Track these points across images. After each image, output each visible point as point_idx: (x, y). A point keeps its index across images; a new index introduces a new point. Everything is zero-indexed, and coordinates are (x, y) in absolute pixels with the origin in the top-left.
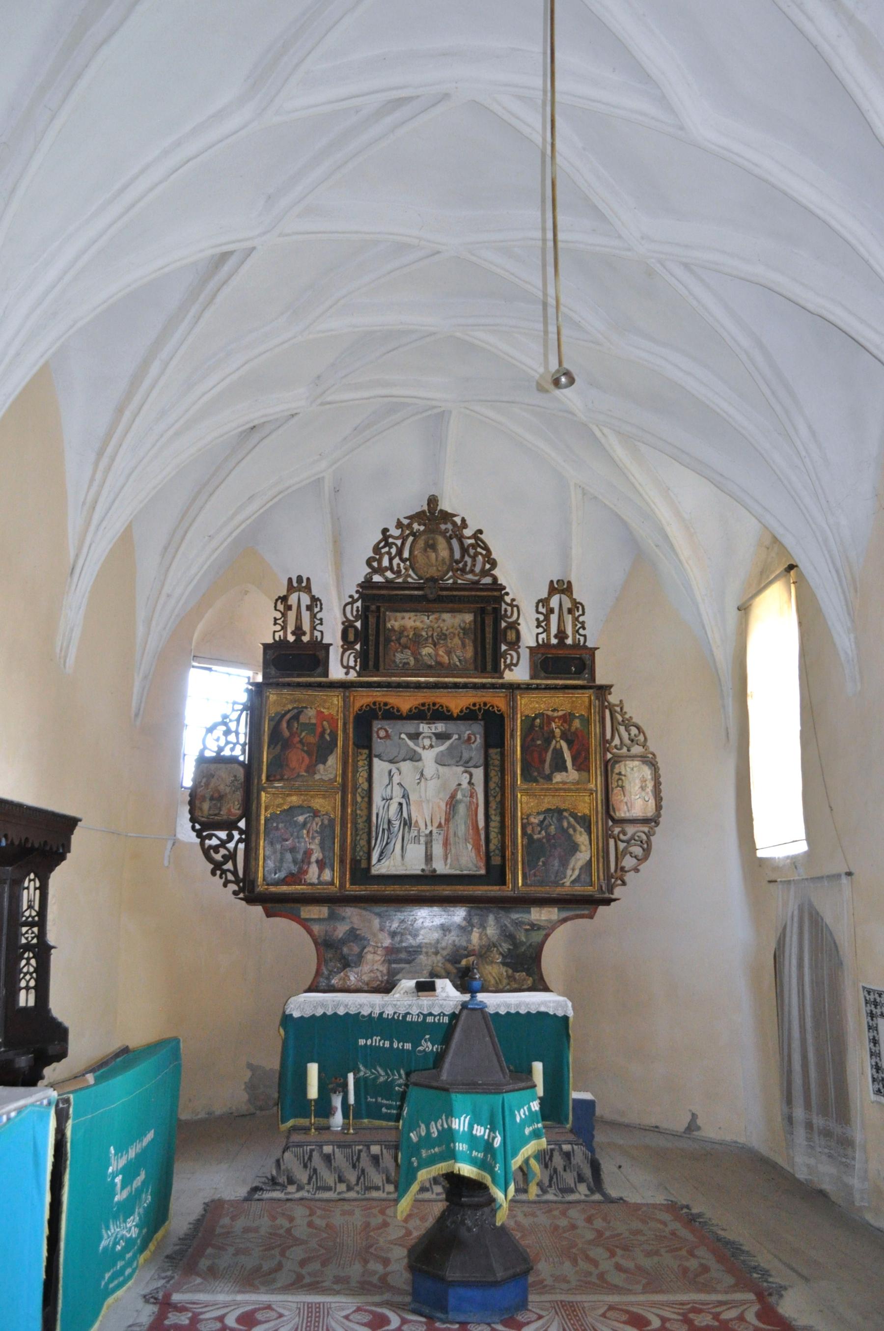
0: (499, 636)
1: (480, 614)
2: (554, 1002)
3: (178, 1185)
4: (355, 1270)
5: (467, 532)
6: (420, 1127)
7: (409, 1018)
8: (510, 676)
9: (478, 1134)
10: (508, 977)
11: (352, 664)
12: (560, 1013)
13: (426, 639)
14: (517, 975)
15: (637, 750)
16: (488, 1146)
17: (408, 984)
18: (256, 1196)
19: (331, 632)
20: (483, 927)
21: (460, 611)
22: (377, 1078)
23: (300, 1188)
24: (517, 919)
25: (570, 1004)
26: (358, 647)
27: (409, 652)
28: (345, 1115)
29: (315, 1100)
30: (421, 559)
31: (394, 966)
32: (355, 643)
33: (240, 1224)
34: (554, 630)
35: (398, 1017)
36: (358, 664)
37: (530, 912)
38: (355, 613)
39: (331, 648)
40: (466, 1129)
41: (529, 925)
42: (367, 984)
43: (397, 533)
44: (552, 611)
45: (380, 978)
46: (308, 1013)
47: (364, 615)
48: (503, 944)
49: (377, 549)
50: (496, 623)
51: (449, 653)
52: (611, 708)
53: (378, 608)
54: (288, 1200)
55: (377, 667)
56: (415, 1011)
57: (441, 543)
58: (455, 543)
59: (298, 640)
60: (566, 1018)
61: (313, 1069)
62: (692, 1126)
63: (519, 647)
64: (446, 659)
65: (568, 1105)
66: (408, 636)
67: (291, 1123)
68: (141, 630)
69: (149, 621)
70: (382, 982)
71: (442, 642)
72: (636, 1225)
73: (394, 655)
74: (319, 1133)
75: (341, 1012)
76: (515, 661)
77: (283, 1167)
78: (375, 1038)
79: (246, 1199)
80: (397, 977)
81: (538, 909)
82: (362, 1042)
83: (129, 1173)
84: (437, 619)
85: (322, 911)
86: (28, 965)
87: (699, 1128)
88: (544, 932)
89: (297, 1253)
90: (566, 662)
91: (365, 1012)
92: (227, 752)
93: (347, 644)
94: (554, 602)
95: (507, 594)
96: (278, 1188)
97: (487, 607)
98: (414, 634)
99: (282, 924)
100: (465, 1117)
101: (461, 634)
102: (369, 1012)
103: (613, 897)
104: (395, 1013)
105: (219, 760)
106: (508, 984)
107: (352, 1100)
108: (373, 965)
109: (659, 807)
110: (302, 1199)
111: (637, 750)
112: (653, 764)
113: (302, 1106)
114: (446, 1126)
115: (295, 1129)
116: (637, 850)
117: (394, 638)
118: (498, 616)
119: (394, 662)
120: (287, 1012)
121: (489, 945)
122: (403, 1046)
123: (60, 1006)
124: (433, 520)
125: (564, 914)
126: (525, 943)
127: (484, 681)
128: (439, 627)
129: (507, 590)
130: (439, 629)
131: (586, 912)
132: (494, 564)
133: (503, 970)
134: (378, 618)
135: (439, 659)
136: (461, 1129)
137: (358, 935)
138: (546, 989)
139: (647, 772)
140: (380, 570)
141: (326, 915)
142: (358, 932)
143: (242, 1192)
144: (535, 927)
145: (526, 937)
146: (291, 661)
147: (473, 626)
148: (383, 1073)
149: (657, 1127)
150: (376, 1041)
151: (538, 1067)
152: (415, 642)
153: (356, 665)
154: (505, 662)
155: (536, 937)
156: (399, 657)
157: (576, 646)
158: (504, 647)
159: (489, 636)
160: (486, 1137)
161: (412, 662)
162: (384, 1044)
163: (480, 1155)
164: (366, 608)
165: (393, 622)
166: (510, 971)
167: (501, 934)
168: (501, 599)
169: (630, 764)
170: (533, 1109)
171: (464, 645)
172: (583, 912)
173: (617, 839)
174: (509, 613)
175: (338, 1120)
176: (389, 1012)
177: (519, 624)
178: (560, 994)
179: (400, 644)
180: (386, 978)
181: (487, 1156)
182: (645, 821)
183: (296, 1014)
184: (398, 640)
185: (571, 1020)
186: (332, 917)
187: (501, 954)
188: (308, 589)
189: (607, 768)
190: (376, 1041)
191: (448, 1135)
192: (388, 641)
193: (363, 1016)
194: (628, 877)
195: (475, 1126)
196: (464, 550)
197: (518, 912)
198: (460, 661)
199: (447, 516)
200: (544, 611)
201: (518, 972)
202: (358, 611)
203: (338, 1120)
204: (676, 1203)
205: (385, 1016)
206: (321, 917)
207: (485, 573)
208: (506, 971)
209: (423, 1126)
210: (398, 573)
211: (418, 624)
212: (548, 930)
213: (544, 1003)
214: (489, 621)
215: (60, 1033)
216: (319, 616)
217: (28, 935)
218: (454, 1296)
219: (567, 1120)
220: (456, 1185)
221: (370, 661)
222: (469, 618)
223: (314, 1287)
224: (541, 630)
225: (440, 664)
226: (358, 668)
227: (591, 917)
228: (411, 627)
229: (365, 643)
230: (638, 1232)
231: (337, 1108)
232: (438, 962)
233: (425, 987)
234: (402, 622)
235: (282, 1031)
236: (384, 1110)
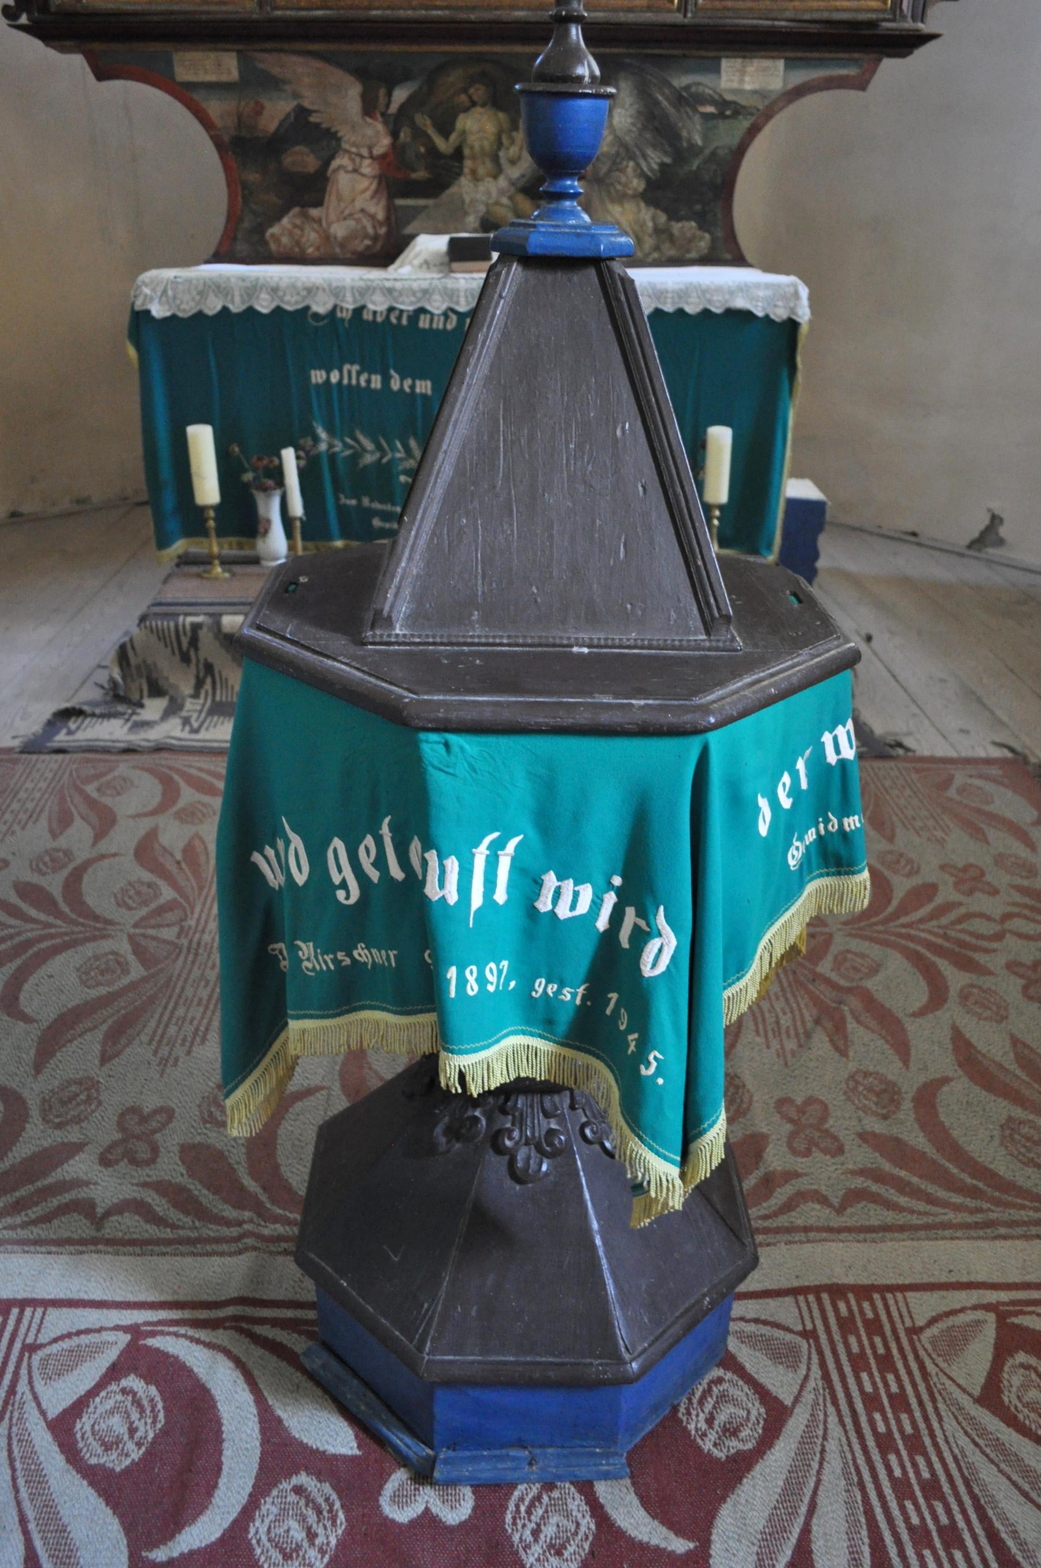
2: (767, 286)
6: (288, 842)
7: (424, 323)
9: (563, 912)
10: (657, 231)
12: (780, 314)
14: (676, 227)
16: (613, 963)
17: (431, 244)
18: (61, 738)
22: (355, 457)
23: (174, 708)
24: (687, 88)
25: (804, 292)
28: (289, 534)
29: (217, 508)
31: (400, 202)
35: (399, 318)
37: (717, 70)
40: (501, 896)
41: (712, 102)
42: (342, 246)
45: (370, 231)
46: (187, 309)
48: (650, 152)
54: (129, 750)
56: (437, 306)
60: (792, 325)
61: (202, 439)
65: (775, 513)
67: (179, 546)
70: (375, 238)
72: (961, 848)
74: (233, 575)
75: (264, 306)
77: (133, 660)
78: (346, 367)
79: (32, 747)
80: (409, 230)
81: (739, 61)
82: (318, 376)
87: (1001, 542)
88: (746, 123)
91: (321, 307)
96: (121, 708)
99: (138, 102)
100: (496, 847)
102: (329, 306)
103: (924, 28)
104: (391, 309)
106: (657, 248)
107: (297, 508)
110: (159, 749)
113: (193, 518)
114: (396, 872)
120: (137, 308)
121: (618, 154)
122: (413, 387)
125: (801, 76)
126: (701, 150)
131: (851, 71)
133: (647, 215)
136: (477, 900)
137: (317, 125)
138: (739, 260)
141: (235, 75)
142: (313, 119)
144: (728, 109)
145: (705, 137)
148: (369, 445)
149: (914, 534)
150: (349, 374)
151: (721, 438)
155: (728, 135)
160: (602, 923)
162: (368, 381)
163: (572, 995)
166: (663, 218)
167: (645, 128)
170: (832, 758)
172: (843, 72)
176: (378, 305)
178: (768, 269)
180: (383, 231)
181: (606, 1004)
183: (158, 311)
185: (804, 329)
186: (255, 82)
187: (642, 175)
190: (349, 375)
191: (405, 916)
193: (316, 316)
195: (551, 880)
197: (687, 71)
201: (679, 219)
203: (277, 543)
204: (1025, 760)
205: (367, 316)
206: (224, 78)
208: (654, 219)
209: (297, 842)
212: (757, 116)
213: (744, 289)
219: (769, 546)
227: (861, 84)
230: (970, 879)
231: (269, 522)
232: (502, 192)
235: (132, 352)
236: (377, 522)
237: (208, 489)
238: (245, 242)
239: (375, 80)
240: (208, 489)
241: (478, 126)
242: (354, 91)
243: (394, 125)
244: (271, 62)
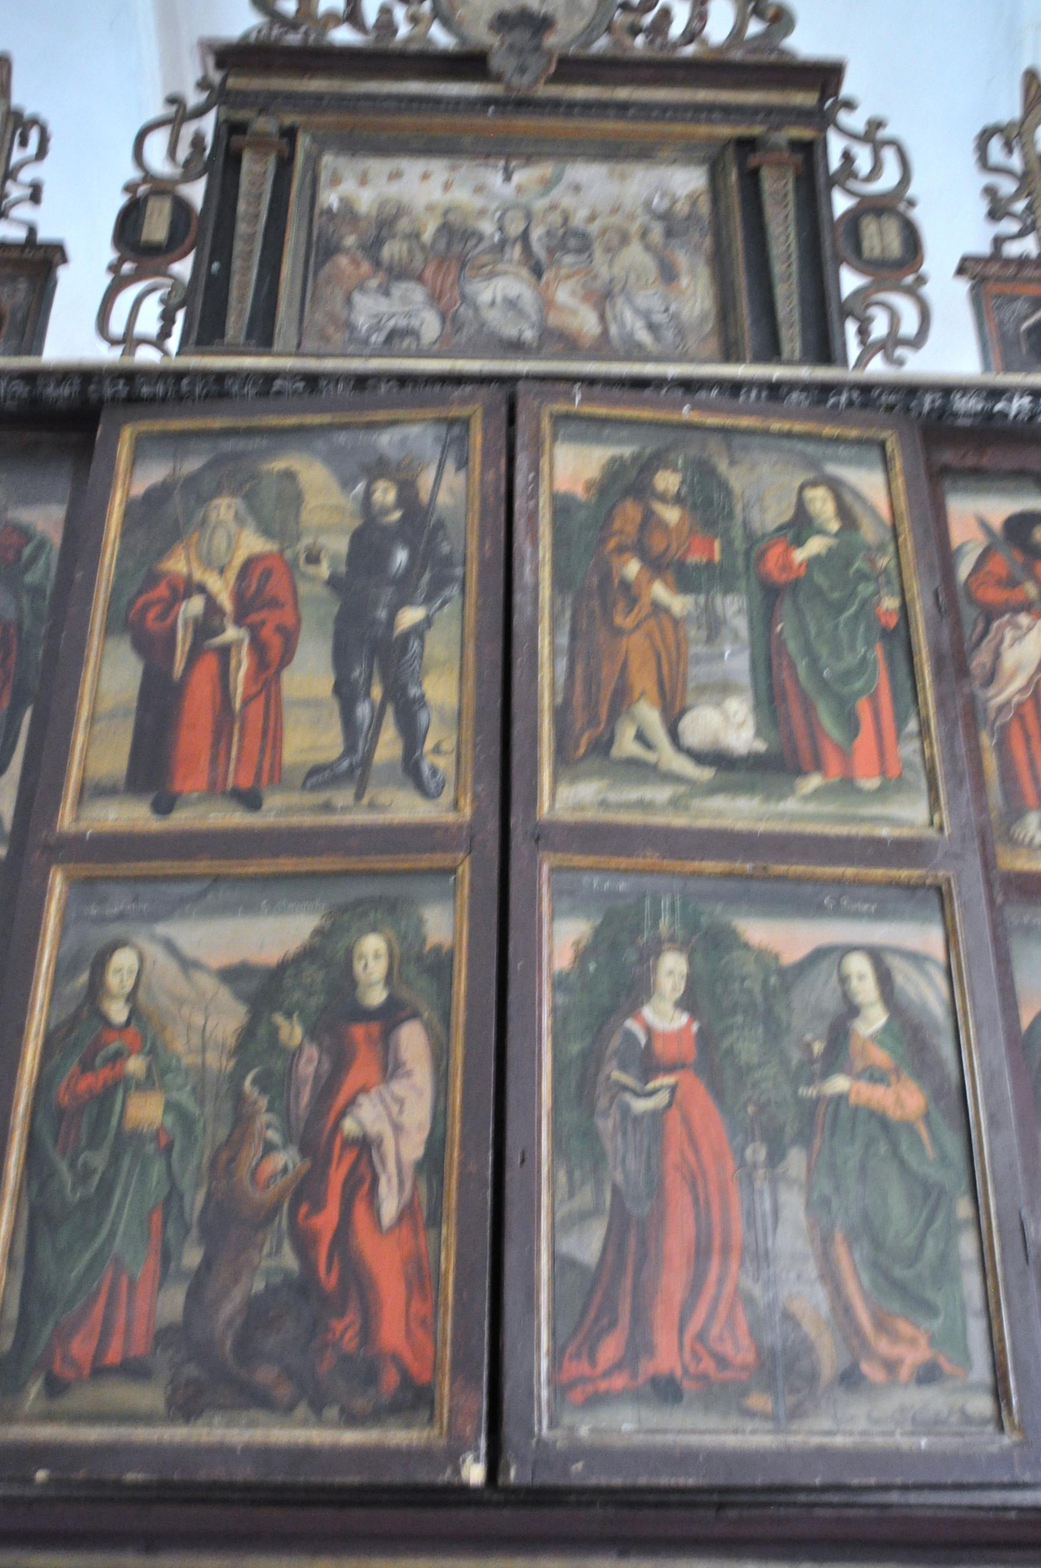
1: (738, 164)
11: (149, 322)
13: (502, 246)
21: (643, 152)
26: (183, 268)
27: (417, 294)
32: (172, 249)
36: (177, 329)
38: (183, 152)
39: (63, 274)
47: (223, 163)
51: (602, 299)
53: (290, 134)
55: (261, 334)
63: (921, 280)
64: (586, 322)
66: (416, 235)
71: (568, 259)
73: (348, 301)
76: (909, 326)
84: (548, 185)
95: (849, 105)
98: (447, 229)
101: (657, 232)
117: (350, 240)
119: (350, 326)
127: (776, 372)
128: (553, 207)
129: (847, 89)
130: (555, 218)
134: (285, 165)
135: (554, 320)
147: (704, 208)
152: (442, 261)
153: (165, 333)
154: (863, 332)
156: (369, 309)
158: (850, 281)
161: (430, 326)
165: (349, 186)
171: (668, 274)
174: (863, 161)
177: (911, 203)
179: (377, 264)
184: (372, 247)
192: (322, 250)
198: (652, 328)
200: (1016, 162)
202: (197, 142)
211: (462, 196)
216: (26, 175)
224: (1010, 226)
225: (558, 340)
226: (173, 343)
228: (430, 208)
234: (393, 190)
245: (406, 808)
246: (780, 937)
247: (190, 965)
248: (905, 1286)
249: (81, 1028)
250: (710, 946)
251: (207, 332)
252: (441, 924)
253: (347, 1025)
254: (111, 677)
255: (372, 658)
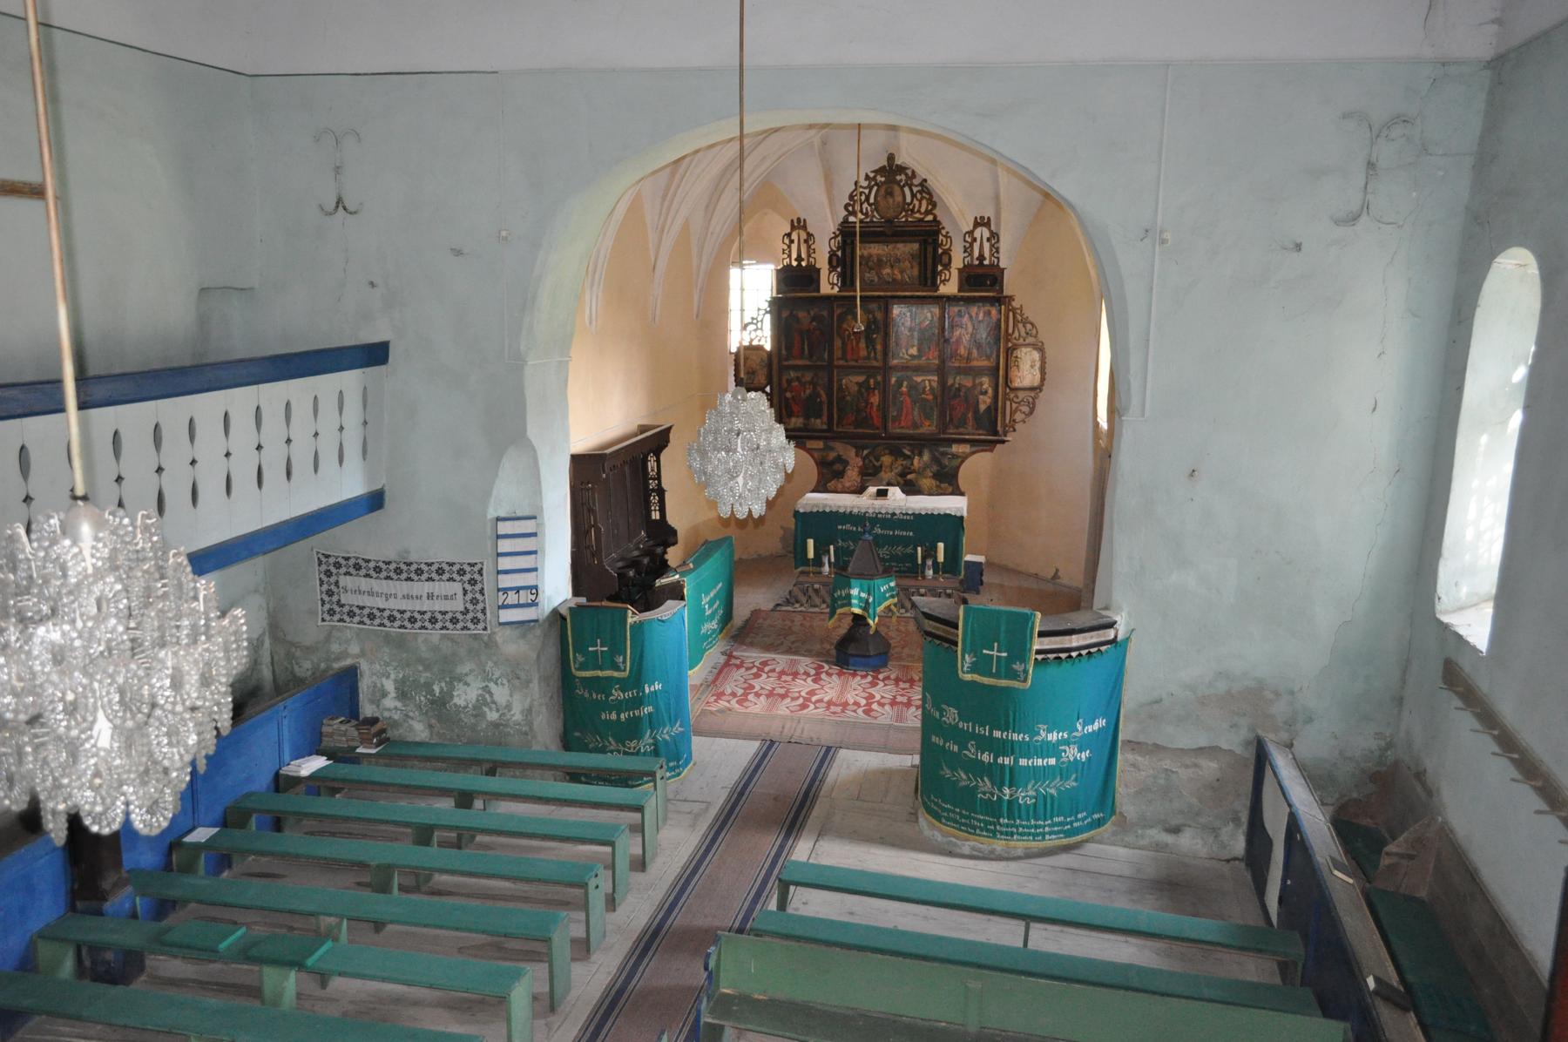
0: (937, 259)
1: (924, 244)
3: (737, 601)
4: (817, 647)
5: (916, 182)
8: (944, 290)
15: (1030, 340)
17: (872, 490)
19: (822, 262)
20: (920, 455)
30: (882, 203)
33: (768, 622)
34: (976, 254)
43: (865, 184)
44: (975, 240)
47: (843, 247)
49: (851, 197)
50: (935, 250)
51: (901, 272)
52: (1014, 310)
57: (897, 189)
58: (907, 190)
59: (799, 265)
61: (811, 542)
62: (1056, 576)
68: (695, 262)
69: (700, 256)
83: (711, 603)
85: (820, 444)
86: (654, 499)
89: (792, 638)
90: (984, 281)
92: (755, 343)
93: (832, 268)
94: (977, 234)
97: (928, 238)
105: (752, 349)
108: (852, 475)
109: (1043, 379)
111: (1030, 340)
112: (1040, 349)
113: (806, 561)
115: (802, 573)
116: (1026, 409)
118: (936, 245)
123: (672, 520)
124: (891, 173)
132: (934, 205)
139: (1036, 355)
140: (854, 213)
143: (771, 606)
144: (955, 456)
146: (796, 282)
150: (848, 527)
155: (955, 462)
157: (992, 265)
159: (930, 261)
164: (844, 242)
168: (938, 232)
169: (1024, 350)
173: (1012, 401)
175: (826, 568)
182: (1032, 389)
186: (828, 448)
188: (804, 227)
189: (1009, 352)
190: (848, 527)
194: (1017, 426)
196: (913, 196)
199: (902, 169)
203: (826, 568)
207: (928, 212)
210: (866, 214)
212: (964, 458)
214: (930, 249)
215: (674, 532)
217: (653, 484)
218: (852, 660)
220: (856, 617)
221: (847, 280)
222: (916, 246)
223: (796, 653)
229: (844, 268)
233: (882, 494)
237: (811, 555)
238: (821, 488)
239: (859, 449)
240: (811, 555)
241: (886, 460)
242: (853, 451)
243: (864, 459)
244: (831, 444)
245: (875, 364)
246: (919, 379)
247: (852, 381)
248: (928, 416)
249: (840, 388)
250: (910, 379)
251: (844, 283)
252: (879, 378)
253: (870, 390)
254: (838, 343)
255: (870, 342)
